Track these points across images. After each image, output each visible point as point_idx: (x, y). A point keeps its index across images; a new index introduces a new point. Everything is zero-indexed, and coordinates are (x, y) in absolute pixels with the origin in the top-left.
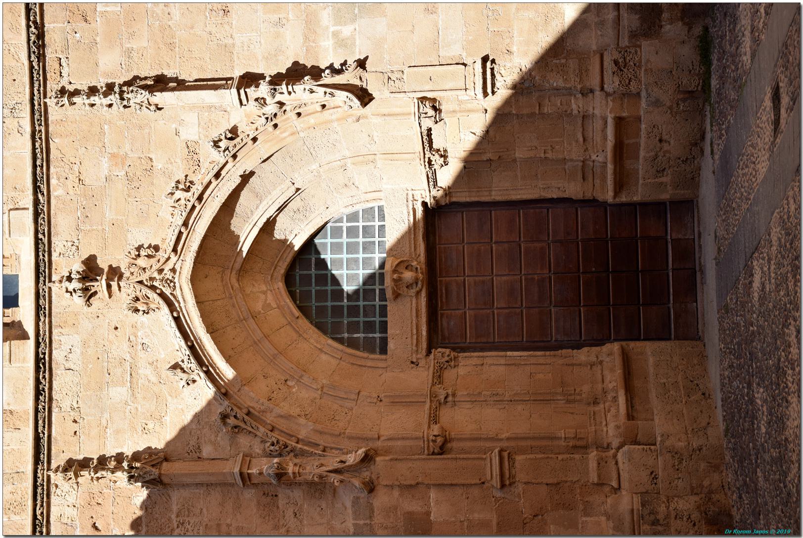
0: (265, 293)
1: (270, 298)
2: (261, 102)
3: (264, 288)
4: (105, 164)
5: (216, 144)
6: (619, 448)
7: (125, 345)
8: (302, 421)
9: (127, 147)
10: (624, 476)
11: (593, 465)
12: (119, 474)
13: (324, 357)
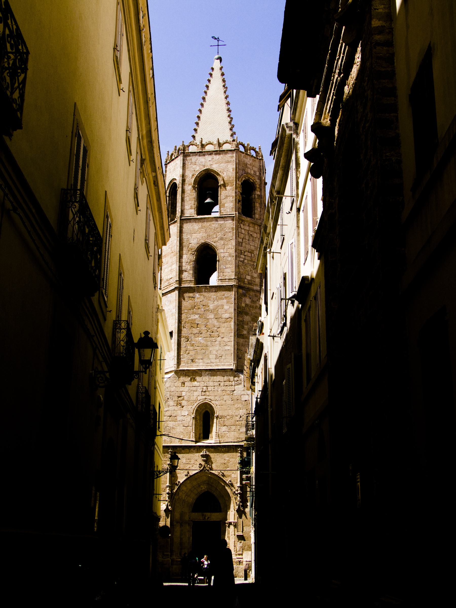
0: (205, 487)
1: (204, 489)
2: (237, 490)
3: (205, 487)
4: (228, 459)
5: (230, 481)
6: (170, 558)
7: (193, 462)
8: (178, 497)
9: (231, 463)
10: (165, 559)
11: (167, 553)
12: (169, 462)
13: (192, 500)
